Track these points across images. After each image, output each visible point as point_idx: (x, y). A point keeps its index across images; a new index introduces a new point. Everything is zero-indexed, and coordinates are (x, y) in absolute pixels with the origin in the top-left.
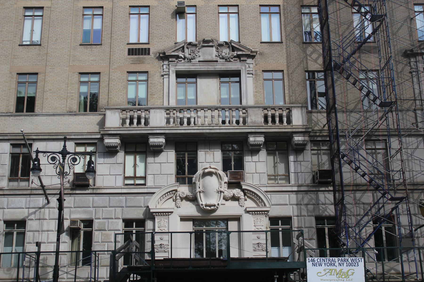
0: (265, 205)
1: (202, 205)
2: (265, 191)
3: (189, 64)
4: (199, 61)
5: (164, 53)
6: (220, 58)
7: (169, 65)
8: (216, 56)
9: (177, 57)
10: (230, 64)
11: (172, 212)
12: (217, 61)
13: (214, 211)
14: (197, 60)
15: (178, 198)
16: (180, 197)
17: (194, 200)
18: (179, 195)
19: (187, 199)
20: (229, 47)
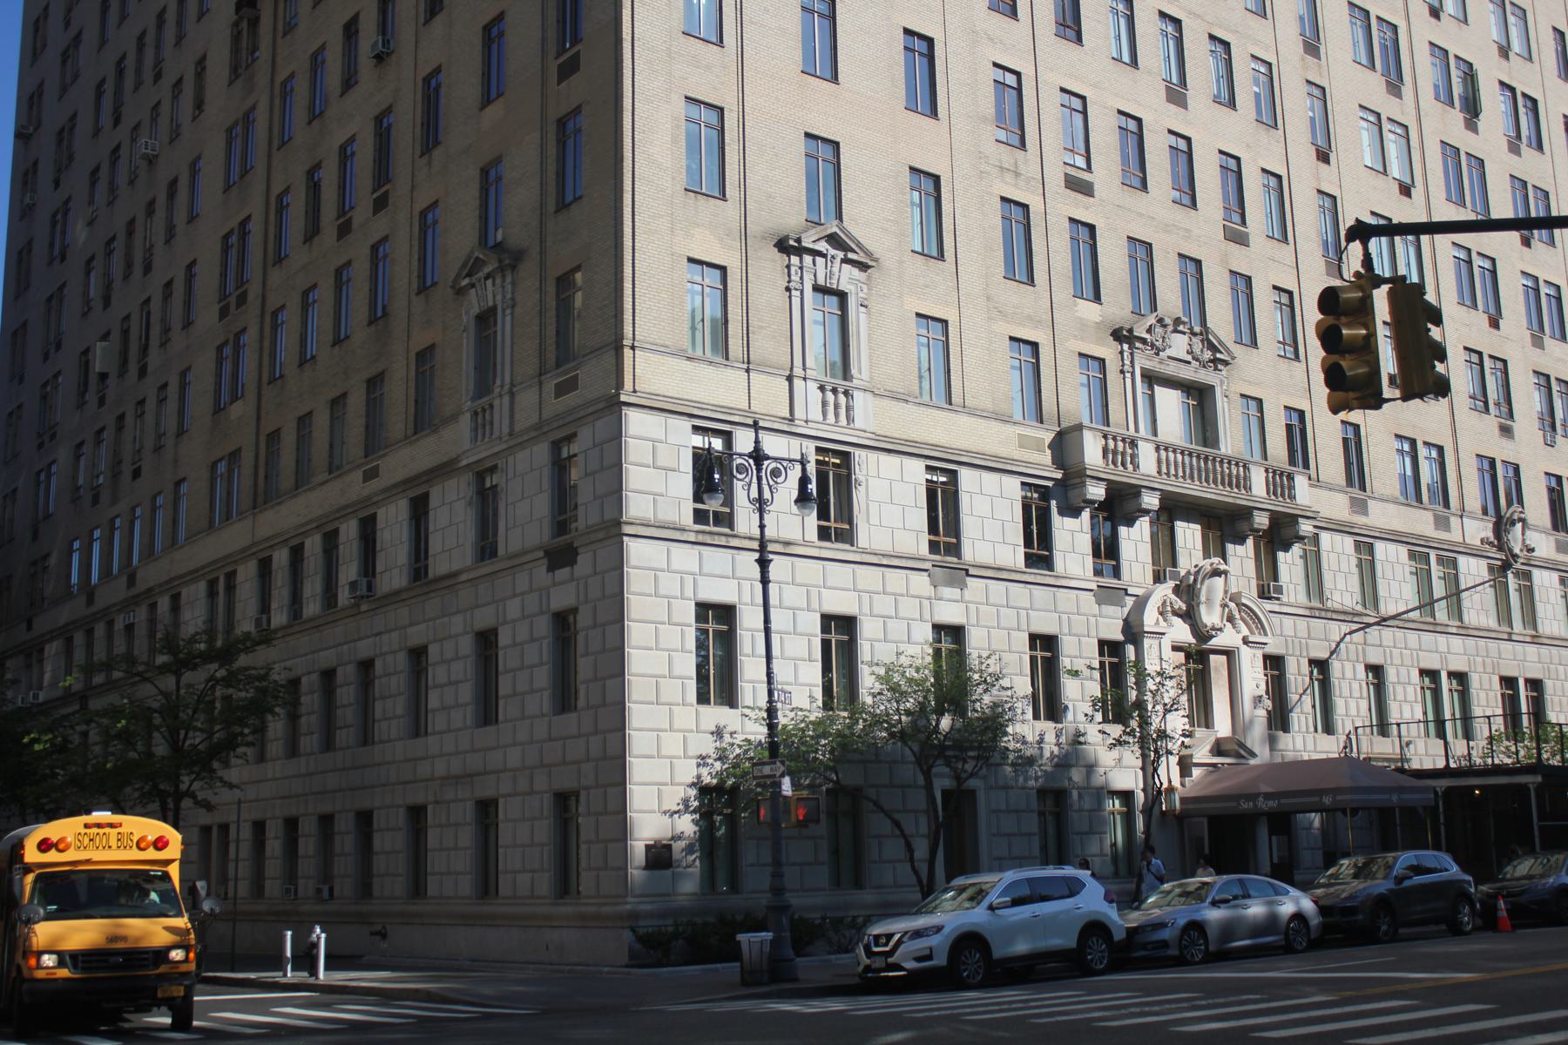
0: (1266, 634)
1: (1206, 626)
2: (1270, 612)
3: (1157, 359)
4: (1169, 357)
5: (1130, 331)
6: (1194, 358)
7: (1132, 354)
8: (1188, 352)
9: (1144, 341)
10: (1202, 371)
11: (1164, 634)
12: (1189, 363)
13: (1212, 637)
14: (1169, 352)
15: (1169, 609)
16: (1172, 607)
17: (1190, 616)
18: (1171, 603)
19: (1175, 613)
20: (1202, 341)
